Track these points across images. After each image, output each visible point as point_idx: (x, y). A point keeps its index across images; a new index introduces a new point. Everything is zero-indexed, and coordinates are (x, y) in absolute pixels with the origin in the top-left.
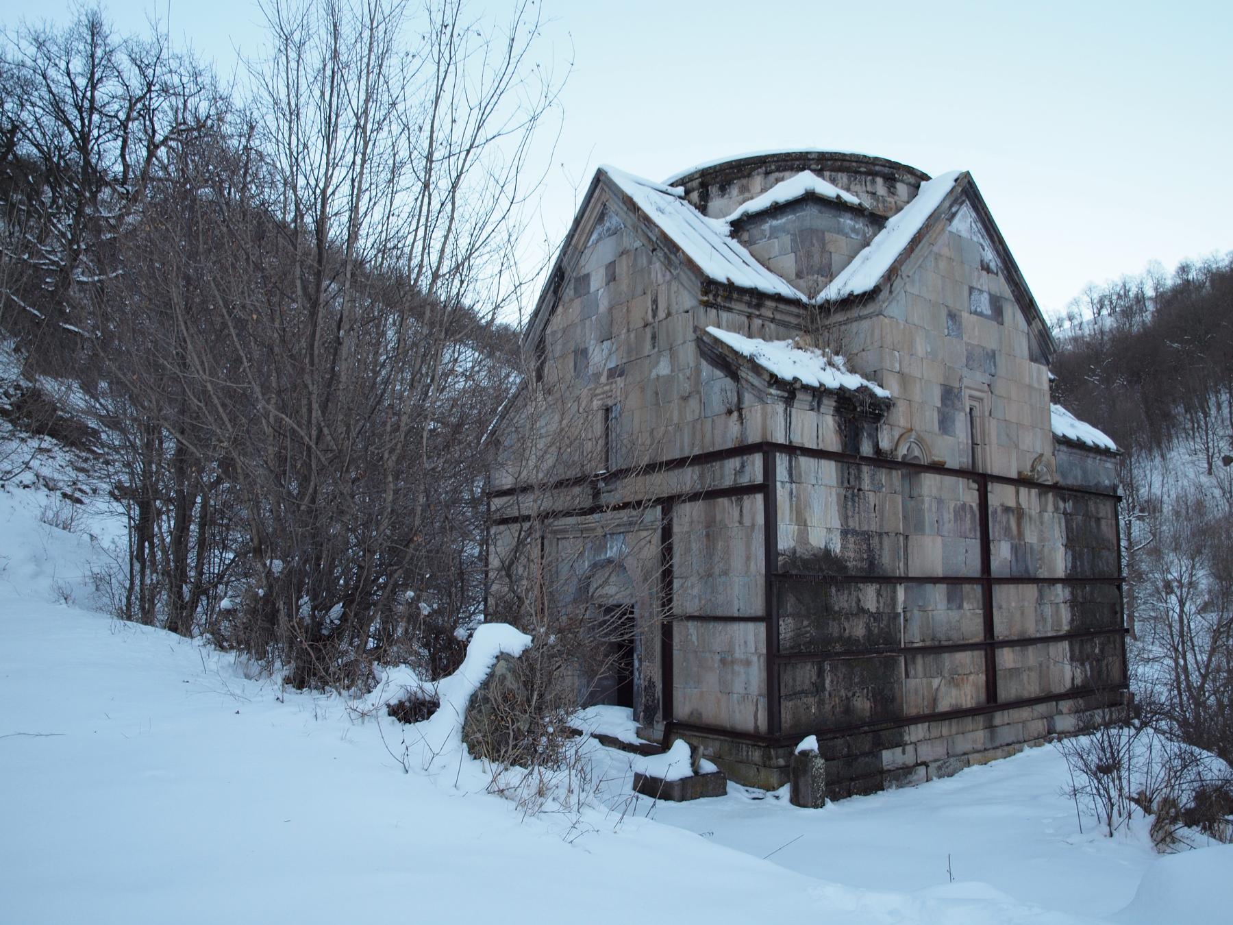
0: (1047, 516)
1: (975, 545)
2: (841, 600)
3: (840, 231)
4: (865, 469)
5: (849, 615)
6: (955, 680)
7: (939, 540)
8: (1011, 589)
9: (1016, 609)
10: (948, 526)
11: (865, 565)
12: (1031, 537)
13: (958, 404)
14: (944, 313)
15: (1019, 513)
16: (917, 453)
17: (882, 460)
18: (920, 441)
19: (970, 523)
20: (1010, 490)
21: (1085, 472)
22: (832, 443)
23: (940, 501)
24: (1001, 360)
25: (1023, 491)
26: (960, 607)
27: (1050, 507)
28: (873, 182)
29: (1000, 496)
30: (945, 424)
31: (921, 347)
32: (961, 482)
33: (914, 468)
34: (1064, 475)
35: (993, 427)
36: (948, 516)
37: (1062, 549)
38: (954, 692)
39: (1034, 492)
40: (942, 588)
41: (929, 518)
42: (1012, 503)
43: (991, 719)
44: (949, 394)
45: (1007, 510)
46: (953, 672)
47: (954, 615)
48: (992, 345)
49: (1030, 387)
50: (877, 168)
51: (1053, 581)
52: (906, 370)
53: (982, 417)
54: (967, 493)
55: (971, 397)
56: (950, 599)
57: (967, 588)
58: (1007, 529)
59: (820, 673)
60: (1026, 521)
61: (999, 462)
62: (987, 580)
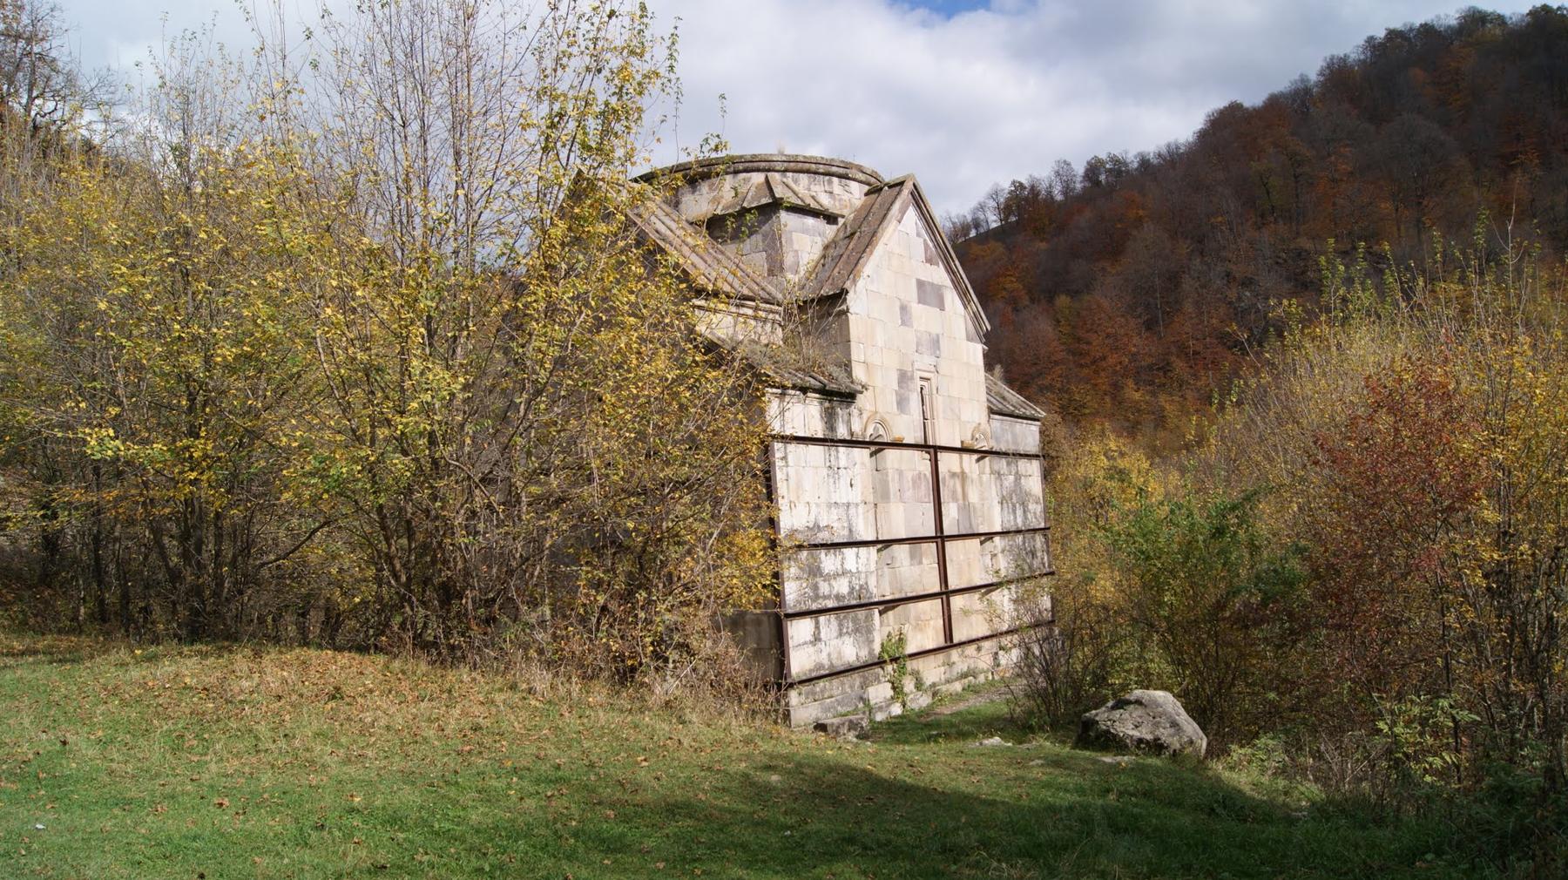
0: (985, 477)
1: (930, 508)
2: (829, 562)
3: (805, 231)
4: (842, 449)
5: (836, 575)
6: (918, 627)
7: (901, 506)
8: (959, 543)
9: (969, 565)
10: (909, 494)
11: (846, 532)
12: (973, 497)
13: (911, 386)
14: (898, 304)
15: (963, 476)
16: (881, 432)
17: (852, 443)
18: (882, 423)
19: (926, 488)
20: (955, 456)
21: (1014, 435)
22: (817, 429)
23: (901, 473)
24: (943, 343)
25: (966, 456)
26: (920, 563)
27: (987, 470)
28: (830, 182)
29: (948, 462)
30: (902, 403)
31: (880, 339)
32: (917, 454)
33: (877, 446)
34: (997, 440)
35: (939, 403)
36: (908, 484)
37: (998, 508)
38: (919, 636)
39: (975, 456)
40: (905, 547)
41: (893, 487)
42: (958, 470)
43: (949, 657)
44: (904, 378)
45: (953, 475)
46: (918, 618)
47: (916, 569)
48: (935, 330)
49: (968, 364)
50: (834, 169)
51: (990, 536)
52: (869, 360)
53: (931, 395)
54: (921, 461)
55: (922, 378)
56: (912, 556)
57: (924, 546)
58: (954, 492)
59: (817, 627)
60: (968, 482)
61: (944, 435)
62: (940, 538)
